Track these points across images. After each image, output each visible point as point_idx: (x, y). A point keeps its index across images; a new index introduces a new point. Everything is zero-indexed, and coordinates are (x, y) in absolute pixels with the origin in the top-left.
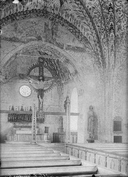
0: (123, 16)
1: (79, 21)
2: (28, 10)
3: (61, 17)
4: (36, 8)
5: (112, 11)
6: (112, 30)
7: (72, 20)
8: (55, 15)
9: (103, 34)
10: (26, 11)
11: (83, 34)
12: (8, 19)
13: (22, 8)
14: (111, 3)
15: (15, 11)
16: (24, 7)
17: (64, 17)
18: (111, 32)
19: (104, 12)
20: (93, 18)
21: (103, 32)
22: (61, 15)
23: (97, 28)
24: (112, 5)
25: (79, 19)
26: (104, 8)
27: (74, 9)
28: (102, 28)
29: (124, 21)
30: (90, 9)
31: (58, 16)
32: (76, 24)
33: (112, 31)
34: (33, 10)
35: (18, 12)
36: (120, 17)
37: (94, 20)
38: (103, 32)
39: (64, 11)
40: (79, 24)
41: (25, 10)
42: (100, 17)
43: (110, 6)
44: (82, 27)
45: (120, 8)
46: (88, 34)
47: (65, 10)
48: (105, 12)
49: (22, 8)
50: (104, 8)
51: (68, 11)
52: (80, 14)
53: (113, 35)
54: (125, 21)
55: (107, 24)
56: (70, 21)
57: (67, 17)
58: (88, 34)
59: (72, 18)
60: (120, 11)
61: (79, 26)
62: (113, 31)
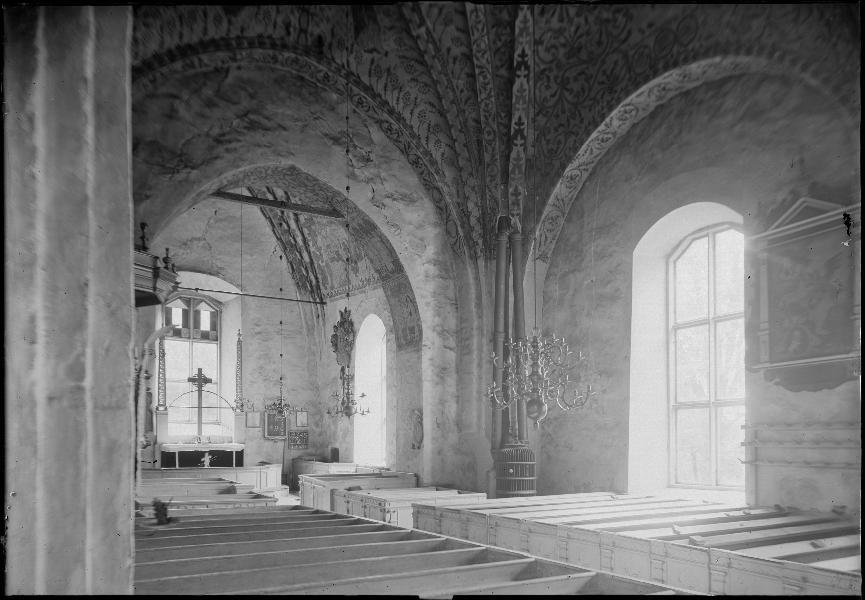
0: (556, 98)
2: (246, 34)
3: (353, 74)
4: (270, 30)
5: (524, 109)
6: (519, 138)
8: (334, 65)
10: (238, 37)
11: (424, 142)
12: (173, 59)
13: (225, 24)
14: (527, 48)
15: (195, 39)
16: (230, 22)
17: (365, 79)
18: (516, 145)
21: (489, 142)
22: (353, 68)
29: (560, 113)
31: (344, 72)
33: (519, 141)
34: (260, 36)
35: (207, 38)
36: (545, 99)
41: (234, 33)
43: (519, 94)
45: (551, 70)
47: (371, 51)
49: (225, 24)
52: (418, 73)
53: (523, 155)
54: (564, 112)
56: (382, 93)
57: (374, 80)
59: (389, 84)
60: (548, 78)
62: (523, 141)
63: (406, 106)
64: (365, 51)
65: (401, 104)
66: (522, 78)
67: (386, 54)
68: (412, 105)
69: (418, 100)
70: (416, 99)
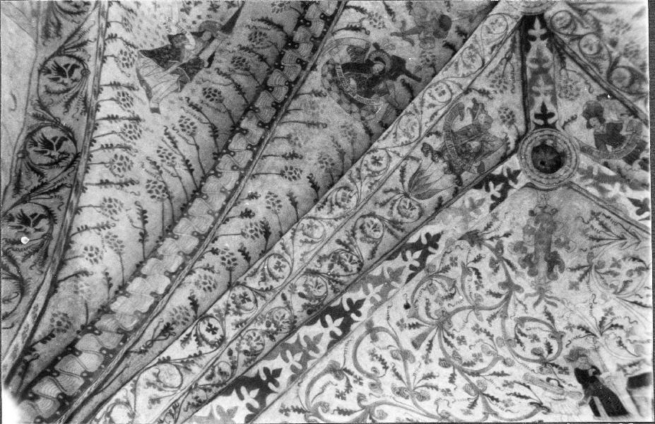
1: (128, 175)
7: (118, 126)
9: (193, 343)
19: (284, 297)
20: (215, 252)
23: (180, 299)
24: (359, 314)
25: (142, 173)
26: (301, 289)
27: (173, 133)
28: (214, 323)
30: (247, 214)
32: (106, 156)
37: (210, 259)
38: (200, 339)
39: (132, 71)
40: (112, 179)
42: (264, 279)
44: (109, 206)
46: (94, 256)
48: (289, 307)
50: (301, 289)
51: (141, 93)
52: (171, 169)
55: (246, 352)
58: (94, 256)
61: (104, 183)
63: (110, 165)
64: (138, 71)
65: (106, 156)
66: (327, 331)
67: (155, 110)
68: (116, 180)
69: (131, 188)
70: (132, 182)
